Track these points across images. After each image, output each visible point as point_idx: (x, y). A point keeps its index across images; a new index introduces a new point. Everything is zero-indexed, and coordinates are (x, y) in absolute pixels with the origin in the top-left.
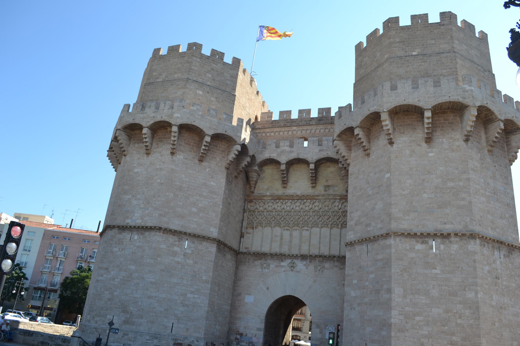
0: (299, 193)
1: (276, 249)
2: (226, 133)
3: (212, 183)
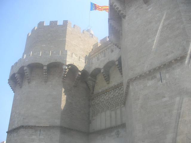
0: (116, 84)
1: (108, 125)
2: (56, 61)
3: (54, 93)
